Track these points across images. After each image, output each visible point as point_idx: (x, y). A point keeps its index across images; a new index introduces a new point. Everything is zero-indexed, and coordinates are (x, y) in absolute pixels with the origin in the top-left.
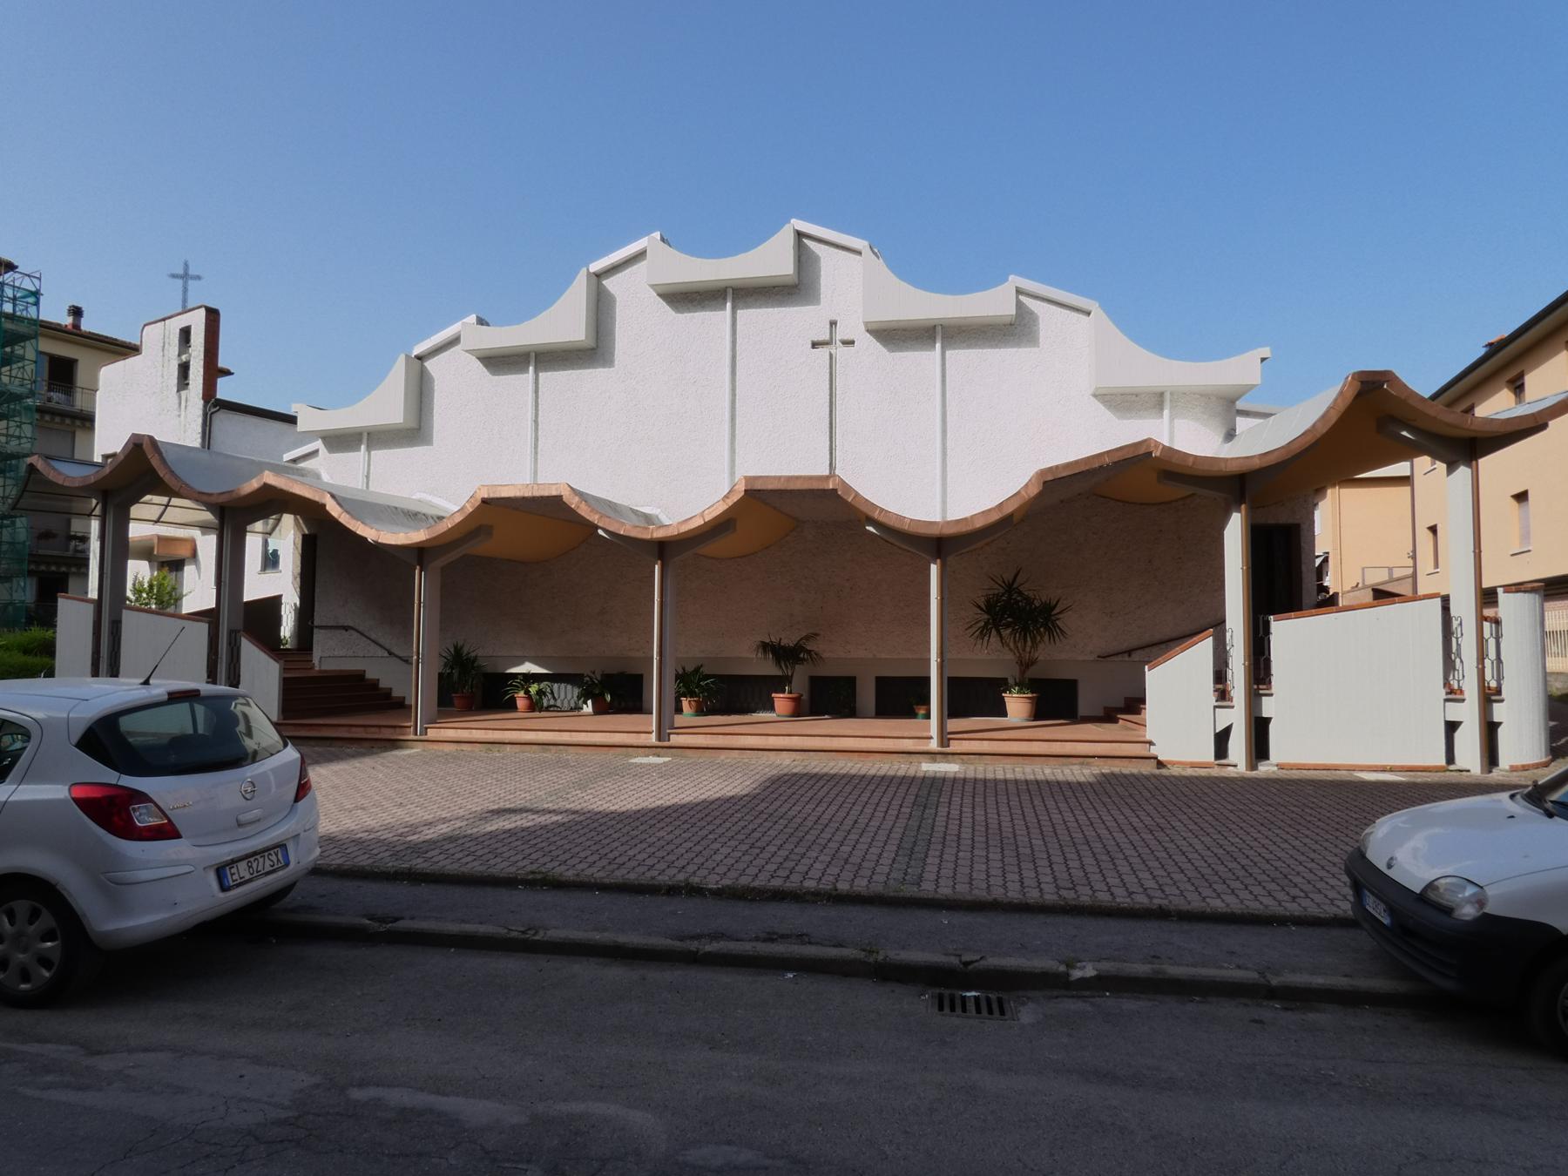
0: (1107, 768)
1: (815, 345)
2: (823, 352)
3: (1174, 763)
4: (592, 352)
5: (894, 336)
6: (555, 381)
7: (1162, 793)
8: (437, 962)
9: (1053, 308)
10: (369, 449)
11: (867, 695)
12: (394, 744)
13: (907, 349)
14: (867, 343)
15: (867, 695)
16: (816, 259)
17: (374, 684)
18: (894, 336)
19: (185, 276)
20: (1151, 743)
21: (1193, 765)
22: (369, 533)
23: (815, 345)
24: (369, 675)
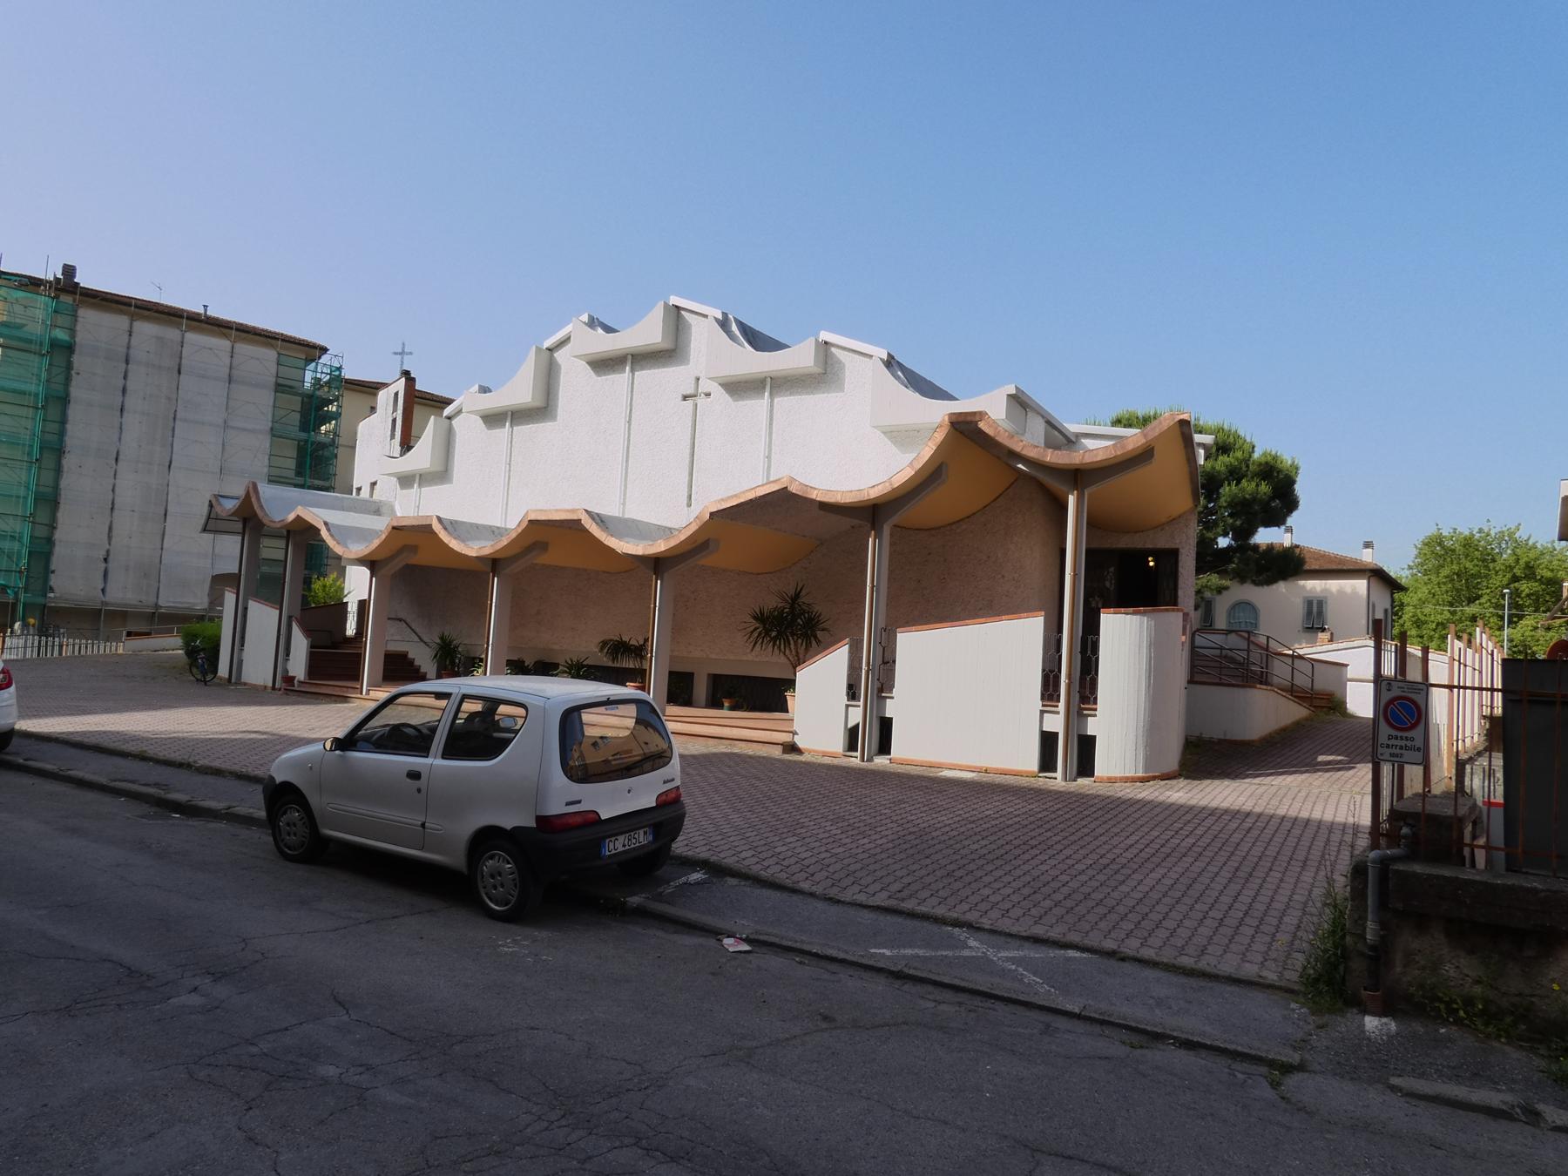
0: (722, 748)
1: (685, 398)
2: (690, 402)
3: (810, 752)
4: (541, 411)
5: (739, 388)
6: (524, 430)
7: (792, 771)
8: (26, 780)
9: (856, 356)
10: (420, 486)
11: (701, 689)
12: (345, 699)
13: (748, 398)
14: (718, 392)
15: (701, 689)
16: (689, 326)
17: (411, 662)
18: (739, 388)
19: (402, 353)
20: (794, 733)
21: (825, 755)
22: (454, 544)
23: (685, 398)
24: (410, 656)
